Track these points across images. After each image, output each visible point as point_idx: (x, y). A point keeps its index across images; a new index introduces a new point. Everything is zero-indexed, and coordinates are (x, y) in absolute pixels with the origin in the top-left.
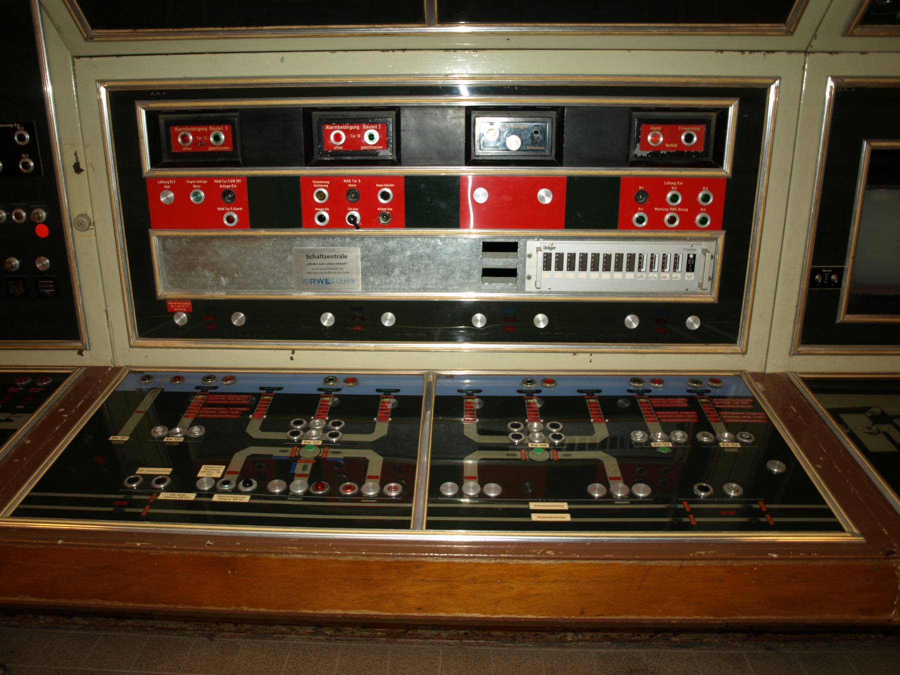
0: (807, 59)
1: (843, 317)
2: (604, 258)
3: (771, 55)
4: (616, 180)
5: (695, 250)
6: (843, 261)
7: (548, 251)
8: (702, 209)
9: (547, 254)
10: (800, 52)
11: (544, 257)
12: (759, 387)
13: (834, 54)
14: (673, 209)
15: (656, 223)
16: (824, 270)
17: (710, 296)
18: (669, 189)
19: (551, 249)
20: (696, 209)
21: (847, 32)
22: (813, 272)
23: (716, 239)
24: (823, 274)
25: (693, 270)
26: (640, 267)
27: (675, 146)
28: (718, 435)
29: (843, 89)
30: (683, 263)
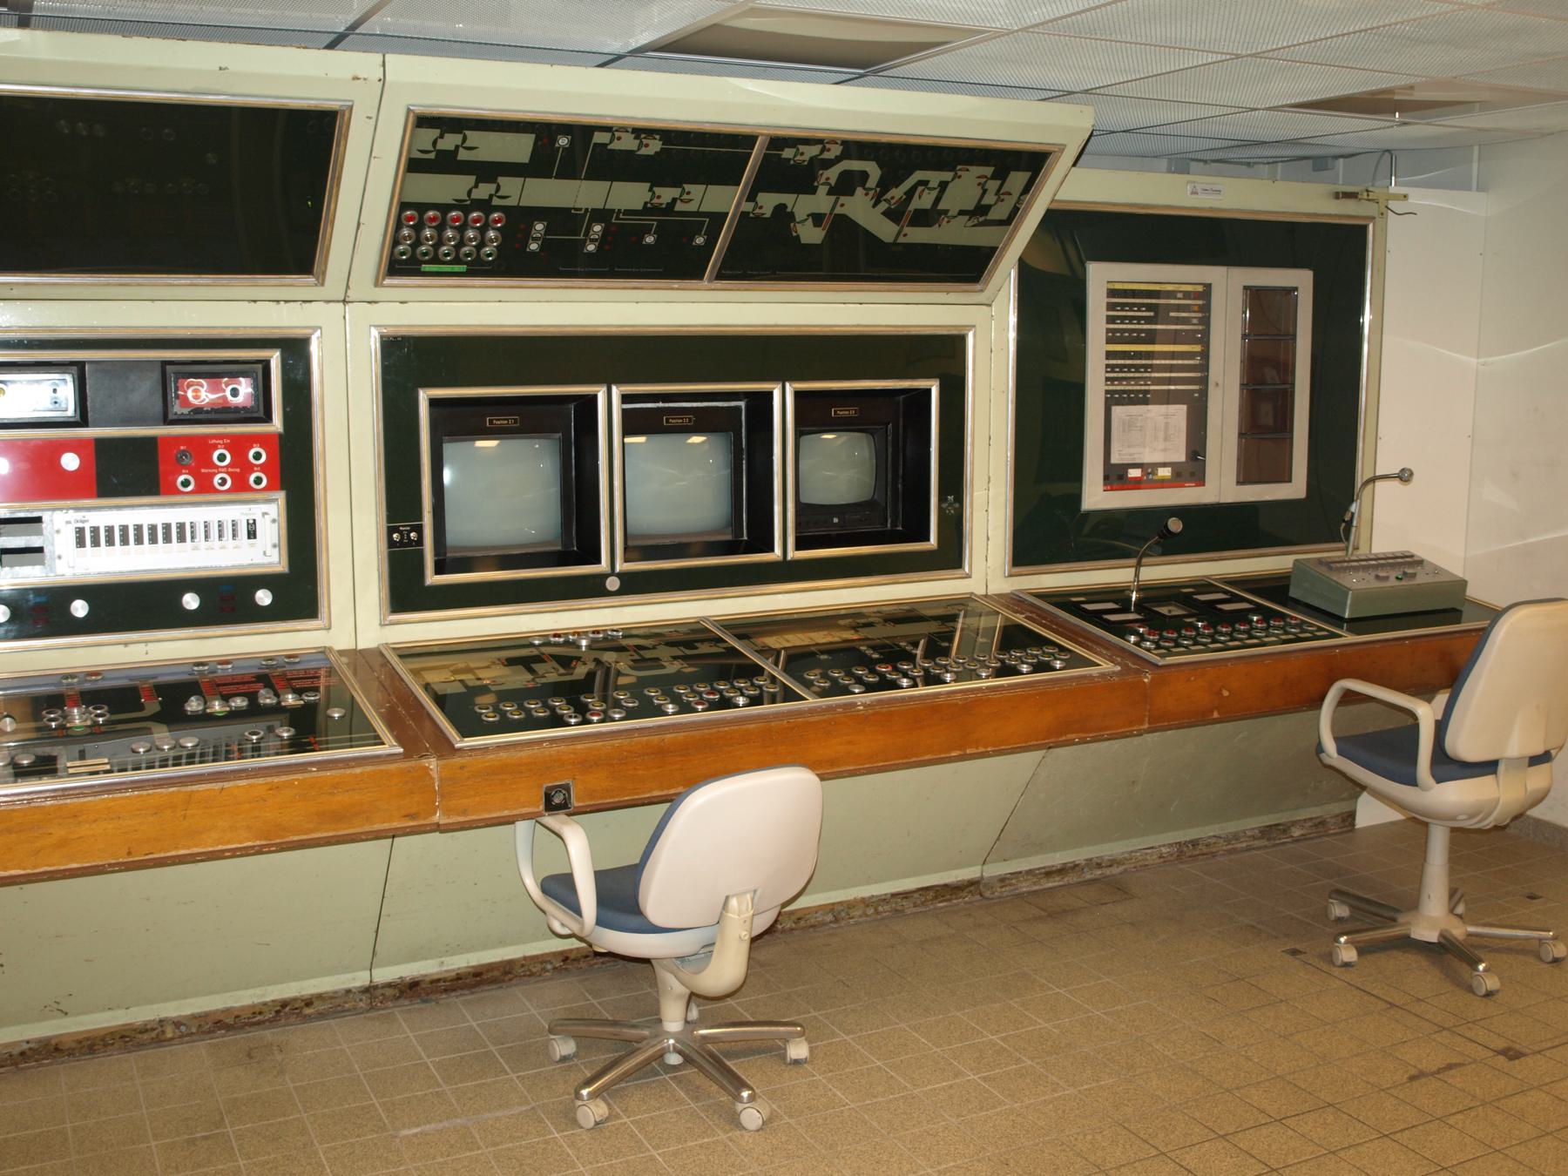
0: (347, 310)
1: (432, 579)
2: (149, 529)
3: (307, 304)
5: (254, 514)
6: (419, 515)
7: (81, 525)
8: (255, 469)
9: (79, 528)
10: (338, 301)
11: (77, 533)
12: (344, 660)
13: (373, 304)
14: (223, 470)
15: (204, 486)
16: (401, 528)
18: (215, 447)
19: (83, 522)
20: (250, 468)
21: (377, 284)
22: (391, 531)
23: (277, 500)
24: (401, 533)
25: (255, 537)
26: (193, 538)
28: (282, 697)
29: (389, 338)
30: (243, 531)
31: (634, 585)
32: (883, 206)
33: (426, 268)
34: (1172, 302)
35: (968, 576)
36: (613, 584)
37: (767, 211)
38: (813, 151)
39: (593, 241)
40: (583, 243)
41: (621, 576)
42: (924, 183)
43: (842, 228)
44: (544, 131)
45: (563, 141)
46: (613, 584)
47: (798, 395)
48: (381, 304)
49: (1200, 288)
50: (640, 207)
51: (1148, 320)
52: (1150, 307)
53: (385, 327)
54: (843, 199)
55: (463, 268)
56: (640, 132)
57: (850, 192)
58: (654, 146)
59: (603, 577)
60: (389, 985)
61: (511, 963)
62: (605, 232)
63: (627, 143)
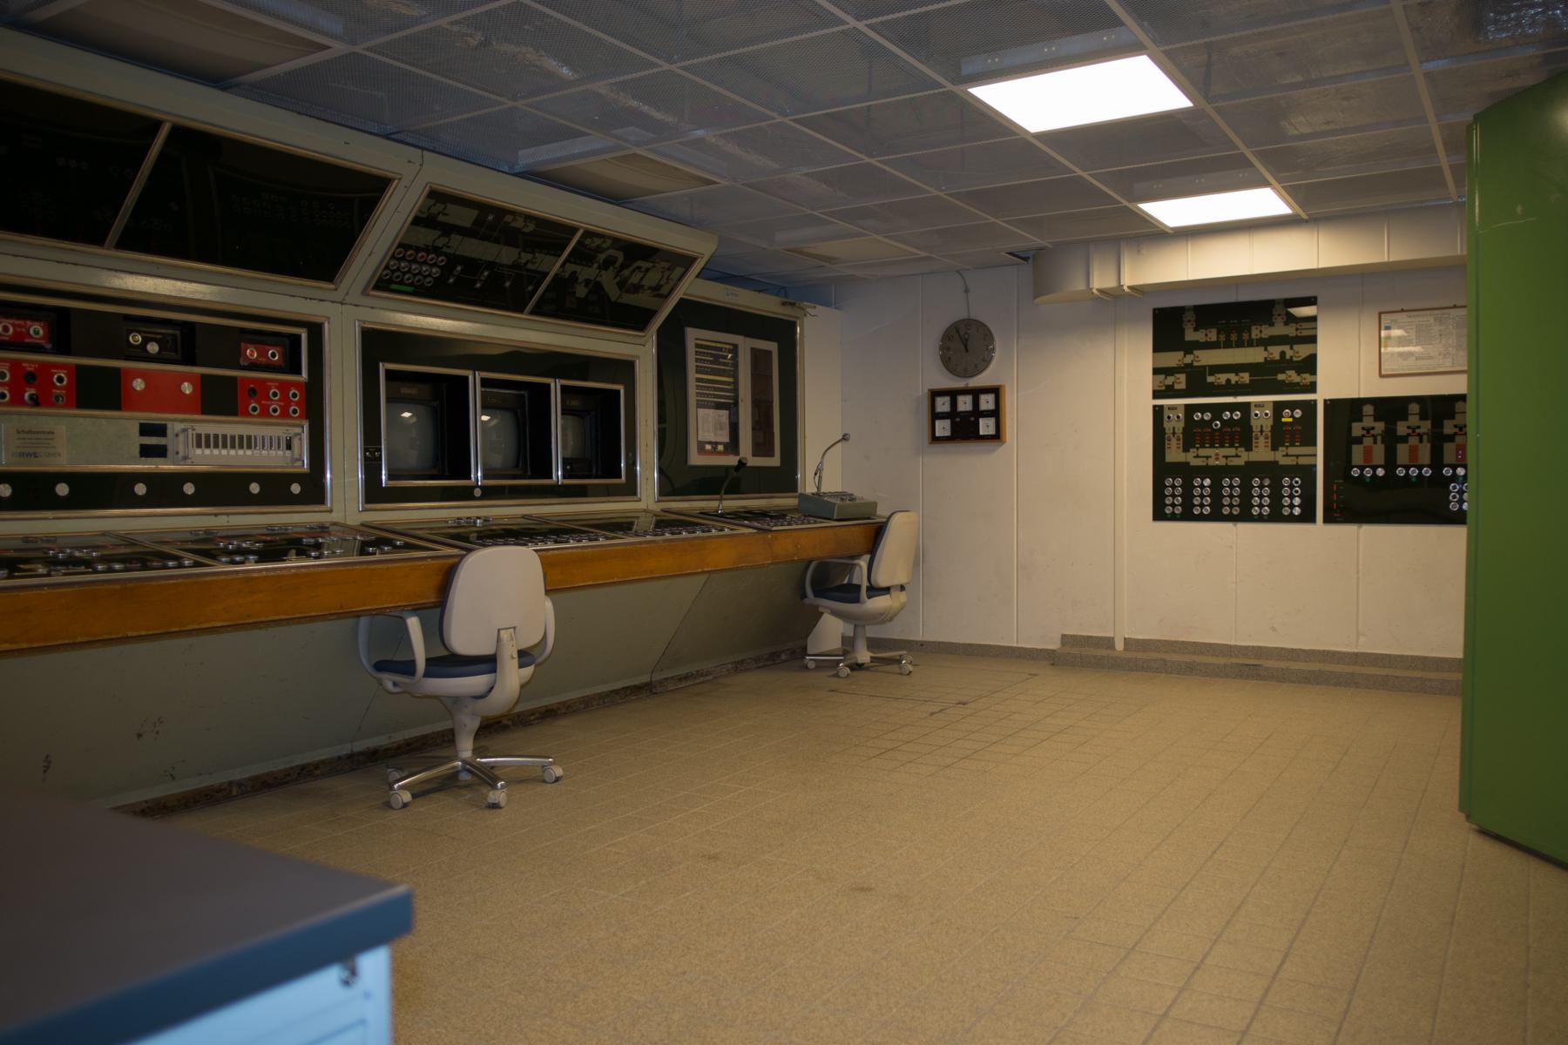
4: (234, 379)
10: (337, 302)
15: (265, 413)
21: (364, 293)
26: (256, 446)
27: (264, 360)
30: (283, 444)
31: (489, 493)
32: (618, 279)
34: (721, 353)
35: (640, 500)
36: (478, 492)
37: (567, 275)
38: (597, 241)
39: (481, 280)
40: (475, 282)
42: (639, 268)
43: (596, 287)
44: (483, 208)
45: (490, 218)
46: (478, 492)
47: (563, 387)
48: (361, 308)
49: (731, 347)
50: (510, 263)
51: (711, 362)
52: (712, 355)
53: (364, 322)
54: (603, 272)
56: (529, 218)
57: (606, 268)
58: (531, 227)
59: (473, 488)
60: (361, 753)
61: (425, 737)
62: (489, 276)
63: (519, 224)
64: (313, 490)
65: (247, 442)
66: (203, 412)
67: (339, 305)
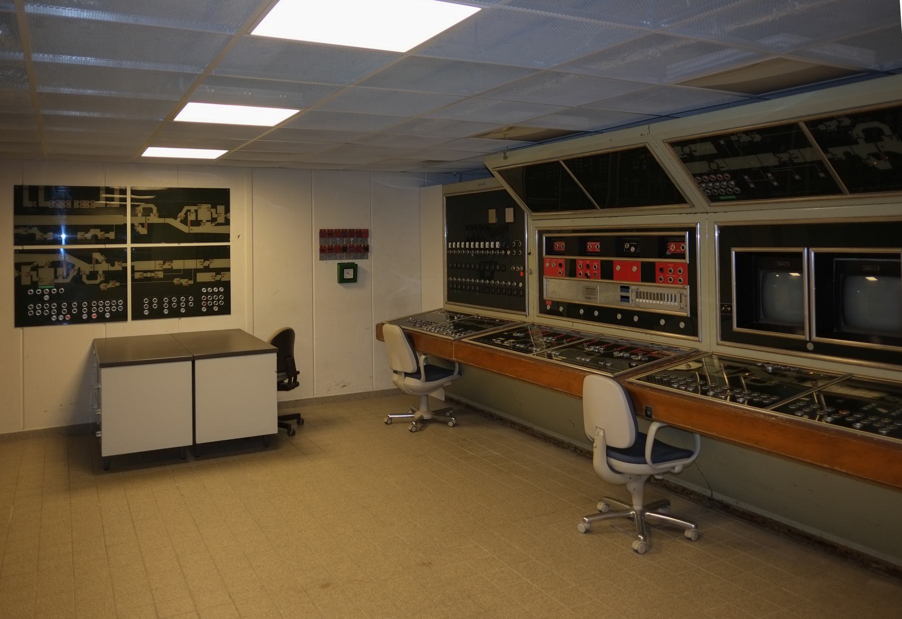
4: (654, 263)
6: (731, 301)
17: (686, 313)
22: (722, 306)
27: (679, 251)
33: (722, 198)
36: (810, 346)
41: (814, 343)
44: (714, 139)
46: (810, 346)
55: (734, 197)
56: (747, 132)
59: (805, 342)
64: (691, 327)
65: (660, 297)
66: (643, 281)
67: (705, 214)
